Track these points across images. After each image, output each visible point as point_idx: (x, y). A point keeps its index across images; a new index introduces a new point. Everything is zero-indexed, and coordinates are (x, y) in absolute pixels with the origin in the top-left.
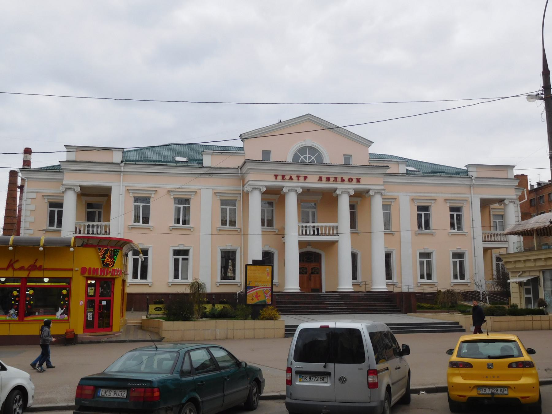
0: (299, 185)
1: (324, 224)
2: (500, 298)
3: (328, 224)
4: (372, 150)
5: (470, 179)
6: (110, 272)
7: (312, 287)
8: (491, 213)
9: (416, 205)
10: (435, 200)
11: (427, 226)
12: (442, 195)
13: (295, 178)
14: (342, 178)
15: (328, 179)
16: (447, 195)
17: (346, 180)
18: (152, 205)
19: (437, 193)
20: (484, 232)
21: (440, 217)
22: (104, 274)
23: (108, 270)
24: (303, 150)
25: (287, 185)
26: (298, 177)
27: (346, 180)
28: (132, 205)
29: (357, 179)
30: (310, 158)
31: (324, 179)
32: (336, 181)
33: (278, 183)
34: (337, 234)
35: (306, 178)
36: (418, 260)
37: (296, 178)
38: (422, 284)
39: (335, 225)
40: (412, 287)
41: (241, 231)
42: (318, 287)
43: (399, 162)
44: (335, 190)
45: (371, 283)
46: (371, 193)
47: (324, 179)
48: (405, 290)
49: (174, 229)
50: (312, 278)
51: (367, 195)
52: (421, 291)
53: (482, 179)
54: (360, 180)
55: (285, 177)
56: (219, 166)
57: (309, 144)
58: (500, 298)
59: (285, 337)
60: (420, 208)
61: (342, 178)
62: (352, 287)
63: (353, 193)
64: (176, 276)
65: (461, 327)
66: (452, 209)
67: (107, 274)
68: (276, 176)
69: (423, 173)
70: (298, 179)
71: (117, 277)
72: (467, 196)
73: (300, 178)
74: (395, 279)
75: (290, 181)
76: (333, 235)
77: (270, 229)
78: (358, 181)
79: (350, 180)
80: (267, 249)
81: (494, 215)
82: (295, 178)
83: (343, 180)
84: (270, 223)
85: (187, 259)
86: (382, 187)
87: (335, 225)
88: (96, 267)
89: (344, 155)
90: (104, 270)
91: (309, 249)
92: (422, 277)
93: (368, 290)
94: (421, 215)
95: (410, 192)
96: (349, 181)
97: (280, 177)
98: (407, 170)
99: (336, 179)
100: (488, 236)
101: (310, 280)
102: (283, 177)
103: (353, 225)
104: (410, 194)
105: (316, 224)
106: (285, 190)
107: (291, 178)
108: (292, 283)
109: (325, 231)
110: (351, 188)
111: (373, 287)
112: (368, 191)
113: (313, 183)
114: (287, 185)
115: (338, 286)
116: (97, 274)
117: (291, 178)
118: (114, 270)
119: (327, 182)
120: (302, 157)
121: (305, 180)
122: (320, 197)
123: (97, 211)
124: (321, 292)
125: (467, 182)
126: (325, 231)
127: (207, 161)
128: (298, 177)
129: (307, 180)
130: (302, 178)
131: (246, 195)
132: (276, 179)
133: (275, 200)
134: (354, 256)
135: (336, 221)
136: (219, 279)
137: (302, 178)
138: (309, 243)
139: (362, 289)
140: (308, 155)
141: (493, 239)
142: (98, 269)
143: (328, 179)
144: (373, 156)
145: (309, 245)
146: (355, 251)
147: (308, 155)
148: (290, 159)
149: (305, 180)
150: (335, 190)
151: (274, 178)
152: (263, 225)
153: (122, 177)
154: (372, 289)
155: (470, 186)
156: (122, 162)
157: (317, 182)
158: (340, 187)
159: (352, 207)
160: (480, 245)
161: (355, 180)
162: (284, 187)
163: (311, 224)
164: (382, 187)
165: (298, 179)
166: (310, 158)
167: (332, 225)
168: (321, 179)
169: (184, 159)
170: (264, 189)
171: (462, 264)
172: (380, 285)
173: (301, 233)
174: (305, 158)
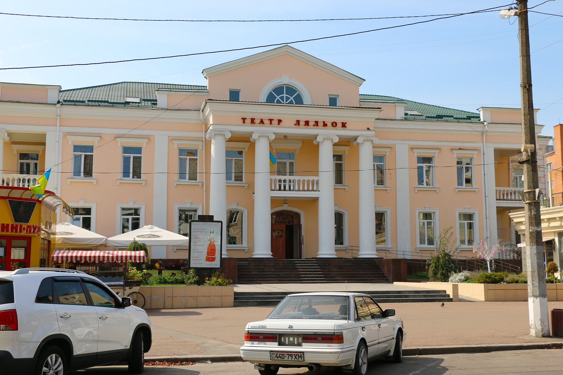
0: (272, 131)
1: (301, 178)
2: (512, 267)
3: (306, 178)
4: (364, 90)
5: (482, 125)
6: (24, 229)
8: (511, 167)
9: (416, 155)
13: (267, 122)
14: (324, 122)
15: (307, 123)
17: (329, 124)
18: (95, 154)
20: (499, 188)
22: (16, 232)
23: (21, 226)
24: (279, 90)
25: (256, 130)
27: (329, 124)
28: (71, 154)
29: (343, 123)
30: (287, 99)
31: (302, 123)
32: (317, 125)
33: (247, 128)
35: (280, 121)
37: (269, 122)
39: (315, 178)
40: (410, 253)
41: (203, 185)
44: (316, 137)
45: (357, 248)
46: (359, 140)
47: (302, 123)
48: (400, 257)
51: (354, 143)
52: (420, 258)
55: (255, 121)
56: (176, 108)
57: (285, 80)
58: (512, 267)
59: (234, 306)
61: (324, 122)
62: (334, 253)
63: (336, 140)
65: (449, 296)
67: (21, 232)
68: (244, 119)
69: (426, 117)
70: (271, 123)
71: (34, 235)
72: (479, 145)
73: (273, 122)
75: (261, 124)
76: (313, 190)
77: (238, 183)
78: (344, 125)
79: (334, 124)
80: (234, 207)
82: (267, 122)
83: (325, 125)
84: (239, 178)
85: (138, 219)
87: (315, 178)
88: (6, 223)
89: (329, 95)
90: (17, 226)
91: (286, 207)
92: (422, 242)
93: (355, 256)
94: (422, 168)
97: (248, 121)
98: (406, 114)
99: (317, 123)
100: (507, 194)
102: (253, 121)
103: (339, 179)
105: (292, 178)
106: (254, 136)
107: (262, 122)
108: (262, 249)
109: (304, 187)
110: (336, 134)
112: (355, 138)
115: (318, 252)
116: (7, 231)
117: (262, 122)
118: (28, 226)
119: (306, 126)
120: (278, 97)
121: (279, 124)
123: (32, 162)
124: (300, 257)
125: (478, 127)
126: (304, 187)
127: (162, 99)
128: (271, 120)
130: (275, 122)
131: (208, 144)
132: (244, 122)
133: (244, 148)
134: (339, 218)
137: (275, 122)
138: (285, 201)
139: (348, 256)
140: (285, 95)
141: (509, 198)
142: (8, 225)
144: (365, 98)
146: (341, 210)
147: (285, 95)
148: (263, 98)
149: (279, 124)
150: (316, 137)
151: (242, 121)
152: (228, 178)
153: (58, 120)
156: (59, 102)
159: (338, 157)
160: (493, 204)
161: (339, 125)
162: (253, 132)
163: (287, 178)
165: (271, 123)
166: (287, 99)
167: (311, 178)
168: (298, 123)
169: (138, 100)
170: (229, 135)
172: (367, 250)
173: (273, 188)
174: (282, 98)
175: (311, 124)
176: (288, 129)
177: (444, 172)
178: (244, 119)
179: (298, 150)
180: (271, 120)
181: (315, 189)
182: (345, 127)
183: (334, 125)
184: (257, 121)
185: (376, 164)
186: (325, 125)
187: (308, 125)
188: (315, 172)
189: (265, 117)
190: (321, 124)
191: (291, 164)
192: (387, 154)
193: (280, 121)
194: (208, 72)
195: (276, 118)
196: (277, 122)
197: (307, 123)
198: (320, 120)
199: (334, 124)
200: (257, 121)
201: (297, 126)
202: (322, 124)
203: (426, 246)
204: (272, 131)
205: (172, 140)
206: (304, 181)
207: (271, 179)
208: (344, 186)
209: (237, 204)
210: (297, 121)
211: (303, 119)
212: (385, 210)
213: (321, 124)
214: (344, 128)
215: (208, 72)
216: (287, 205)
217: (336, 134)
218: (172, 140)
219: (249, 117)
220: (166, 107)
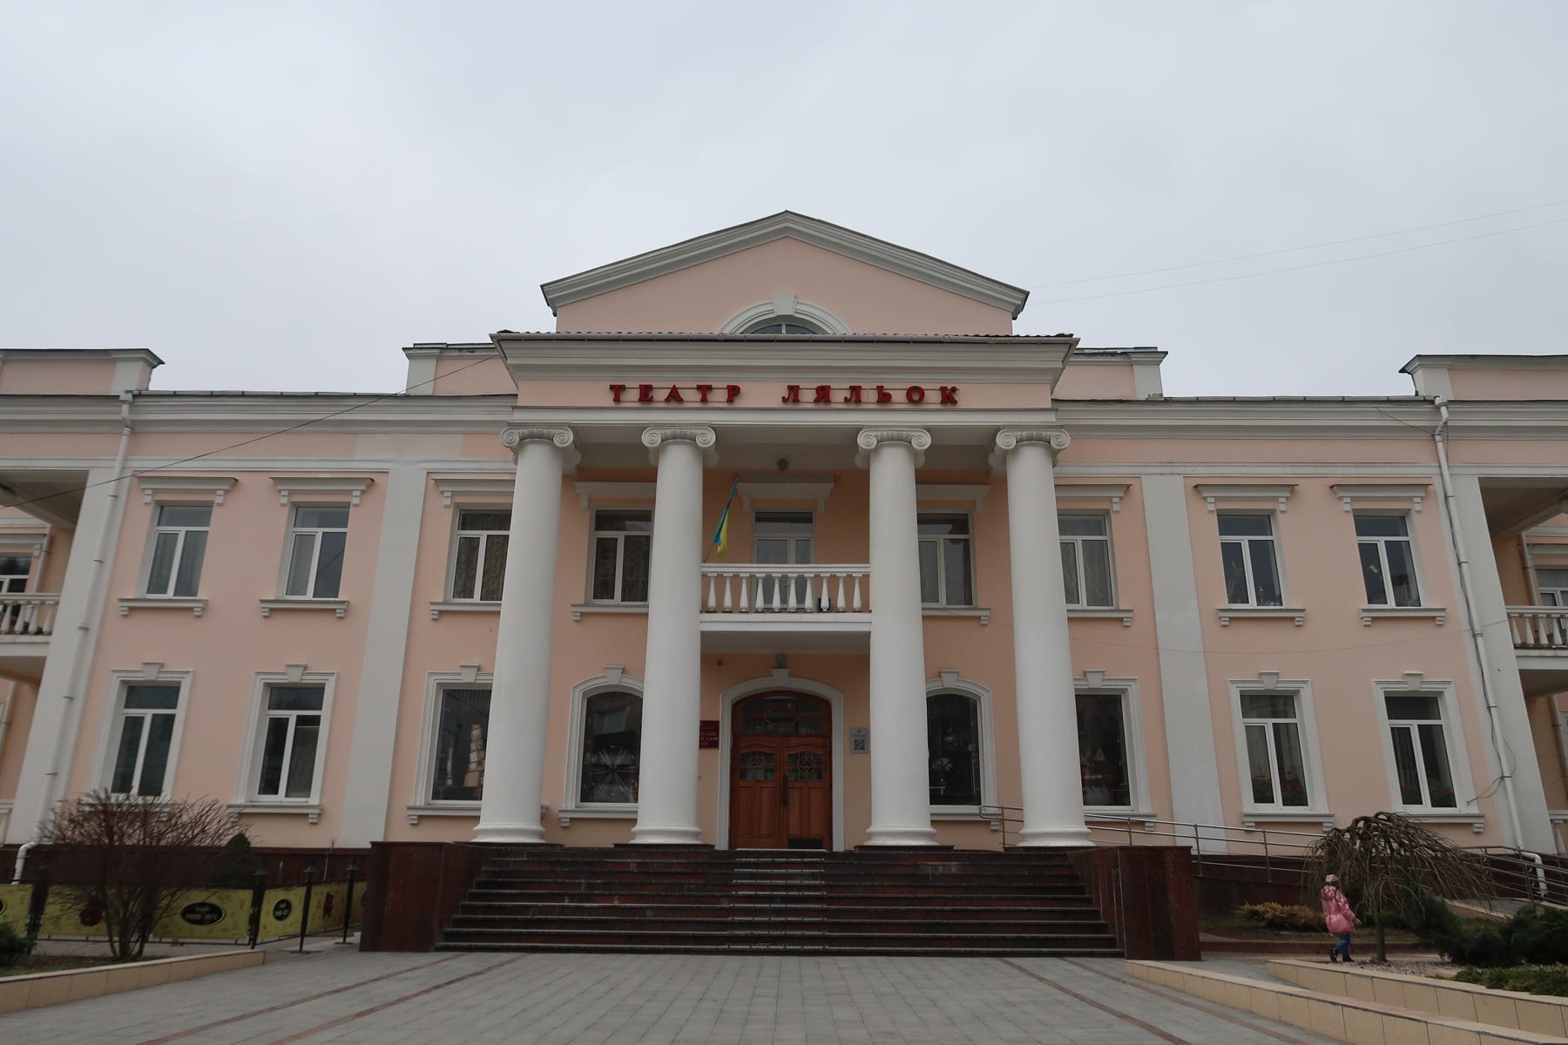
0: (704, 421)
3: (826, 569)
7: (794, 830)
8: (1530, 563)
10: (1291, 488)
11: (1269, 592)
12: (1319, 470)
14: (880, 389)
15: (823, 395)
16: (1339, 471)
17: (899, 396)
19: (1293, 464)
21: (1318, 555)
25: (653, 422)
26: (705, 390)
27: (899, 396)
29: (943, 389)
31: (808, 396)
34: (866, 608)
35: (733, 392)
36: (1239, 723)
37: (697, 396)
38: (1264, 824)
39: (856, 569)
42: (816, 830)
43: (1135, 358)
45: (1011, 815)
47: (808, 396)
49: (275, 610)
50: (795, 797)
52: (1258, 851)
53: (1479, 408)
57: (784, 308)
60: (1228, 522)
61: (880, 389)
63: (925, 441)
64: (269, 784)
66: (1366, 523)
68: (618, 391)
73: (712, 396)
74: (1141, 801)
75: (673, 404)
76: (849, 609)
78: (948, 397)
79: (915, 396)
81: (1540, 570)
83: (884, 397)
85: (316, 720)
86: (1051, 418)
91: (781, 680)
92: (1262, 794)
95: (1187, 464)
96: (910, 399)
97: (632, 396)
101: (785, 803)
102: (646, 394)
104: (1188, 470)
106: (649, 439)
107: (674, 396)
110: (921, 424)
111: (1026, 830)
113: (763, 408)
114: (653, 422)
115: (869, 824)
117: (674, 396)
119: (822, 406)
121: (730, 400)
122: (829, 486)
128: (705, 390)
129: (739, 403)
130: (719, 396)
132: (617, 400)
135: (864, 557)
136: (419, 791)
137: (719, 396)
143: (823, 395)
145: (780, 666)
154: (1024, 837)
155: (1431, 433)
157: (778, 403)
158: (869, 422)
161: (933, 397)
164: (1051, 418)
165: (704, 400)
167: (841, 569)
168: (793, 394)
171: (1432, 739)
173: (712, 603)
175: (838, 396)
177: (1318, 555)
181: (857, 603)
182: (955, 402)
183: (916, 397)
184: (660, 395)
185: (1078, 540)
186: (884, 397)
187: (828, 401)
188: (856, 543)
192: (1116, 507)
194: (557, 294)
196: (723, 395)
200: (660, 395)
202: (874, 396)
203: (1277, 808)
204: (704, 421)
205: (439, 483)
207: (704, 575)
208: (976, 609)
209: (624, 671)
212: (1120, 685)
213: (870, 396)
214: (950, 406)
215: (557, 294)
216: (786, 671)
217: (921, 424)
218: (439, 483)
220: (429, 392)
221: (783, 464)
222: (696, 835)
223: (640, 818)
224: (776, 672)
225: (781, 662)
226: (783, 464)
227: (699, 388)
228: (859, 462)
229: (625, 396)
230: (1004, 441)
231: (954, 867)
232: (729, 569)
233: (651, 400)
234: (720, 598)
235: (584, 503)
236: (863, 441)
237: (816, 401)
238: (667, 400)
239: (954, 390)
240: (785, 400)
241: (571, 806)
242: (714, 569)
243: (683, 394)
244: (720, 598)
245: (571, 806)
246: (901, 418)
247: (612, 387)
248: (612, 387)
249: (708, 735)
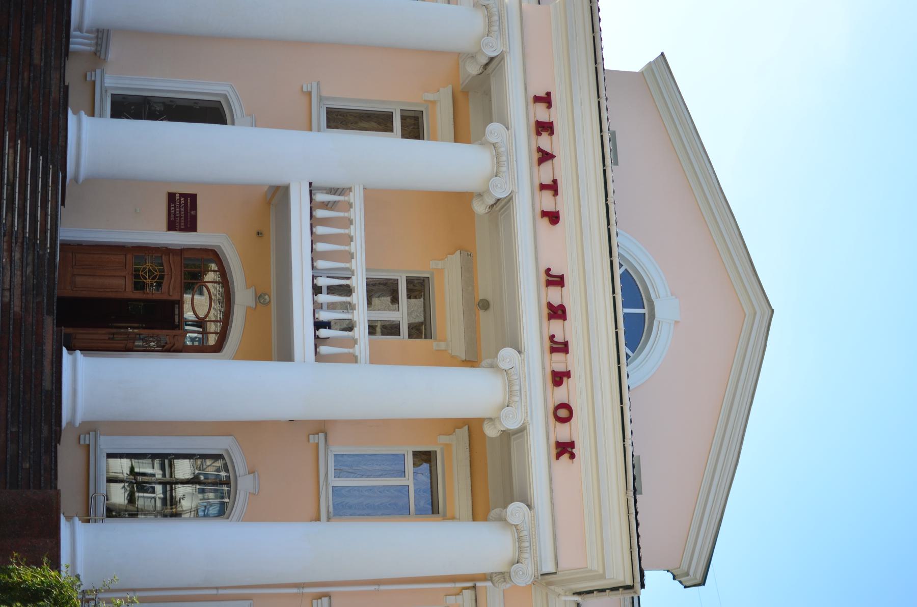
14: (568, 374)
17: (560, 394)
27: (560, 394)
29: (572, 444)
31: (555, 296)
35: (553, 217)
37: (548, 181)
47: (555, 296)
54: (565, 457)
55: (545, 135)
61: (568, 374)
62: (78, 420)
68: (546, 100)
70: (543, 187)
73: (548, 194)
75: (536, 156)
78: (565, 449)
79: (563, 413)
82: (545, 174)
83: (559, 378)
97: (541, 113)
102: (545, 127)
106: (494, 130)
117: (545, 157)
119: (546, 311)
121: (544, 214)
130: (547, 202)
132: (537, 99)
137: (547, 202)
149: (544, 214)
151: (542, 94)
161: (563, 433)
165: (543, 187)
168: (555, 281)
173: (320, 197)
175: (556, 327)
176: (529, 247)
178: (546, 100)
179: (443, 346)
180: (553, 187)
182: (558, 456)
183: (563, 413)
186: (559, 378)
189: (561, 169)
190: (559, 362)
191: (392, 329)
193: (553, 217)
195: (564, 204)
196: (550, 208)
197: (557, 312)
198: (573, 361)
199: (563, 413)
200: (544, 142)
201: (544, 278)
202: (560, 368)
206: (349, 307)
210: (562, 277)
211: (568, 297)
213: (559, 362)
214: (554, 452)
219: (557, 115)
221: (485, 305)
222: (76, 179)
223: (96, 120)
224: (252, 290)
225: (260, 298)
226: (485, 305)
227: (555, 181)
228: (489, 361)
229: (541, 107)
230: (516, 511)
231: (47, 384)
232: (358, 214)
233: (539, 134)
234: (325, 205)
235: (430, 97)
236: (507, 355)
237: (550, 305)
238: (539, 150)
239: (572, 456)
240: (549, 270)
241: (109, 82)
242: (357, 198)
243: (547, 165)
244: (325, 205)
245: (109, 82)
246: (537, 400)
247: (548, 94)
248: (548, 94)
249: (182, 210)
